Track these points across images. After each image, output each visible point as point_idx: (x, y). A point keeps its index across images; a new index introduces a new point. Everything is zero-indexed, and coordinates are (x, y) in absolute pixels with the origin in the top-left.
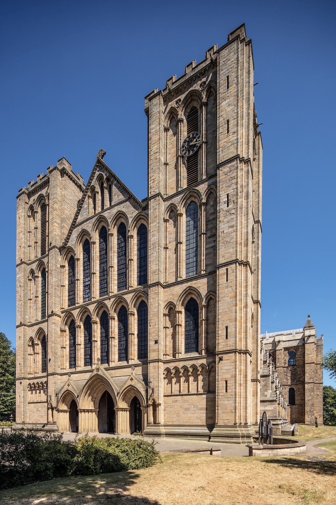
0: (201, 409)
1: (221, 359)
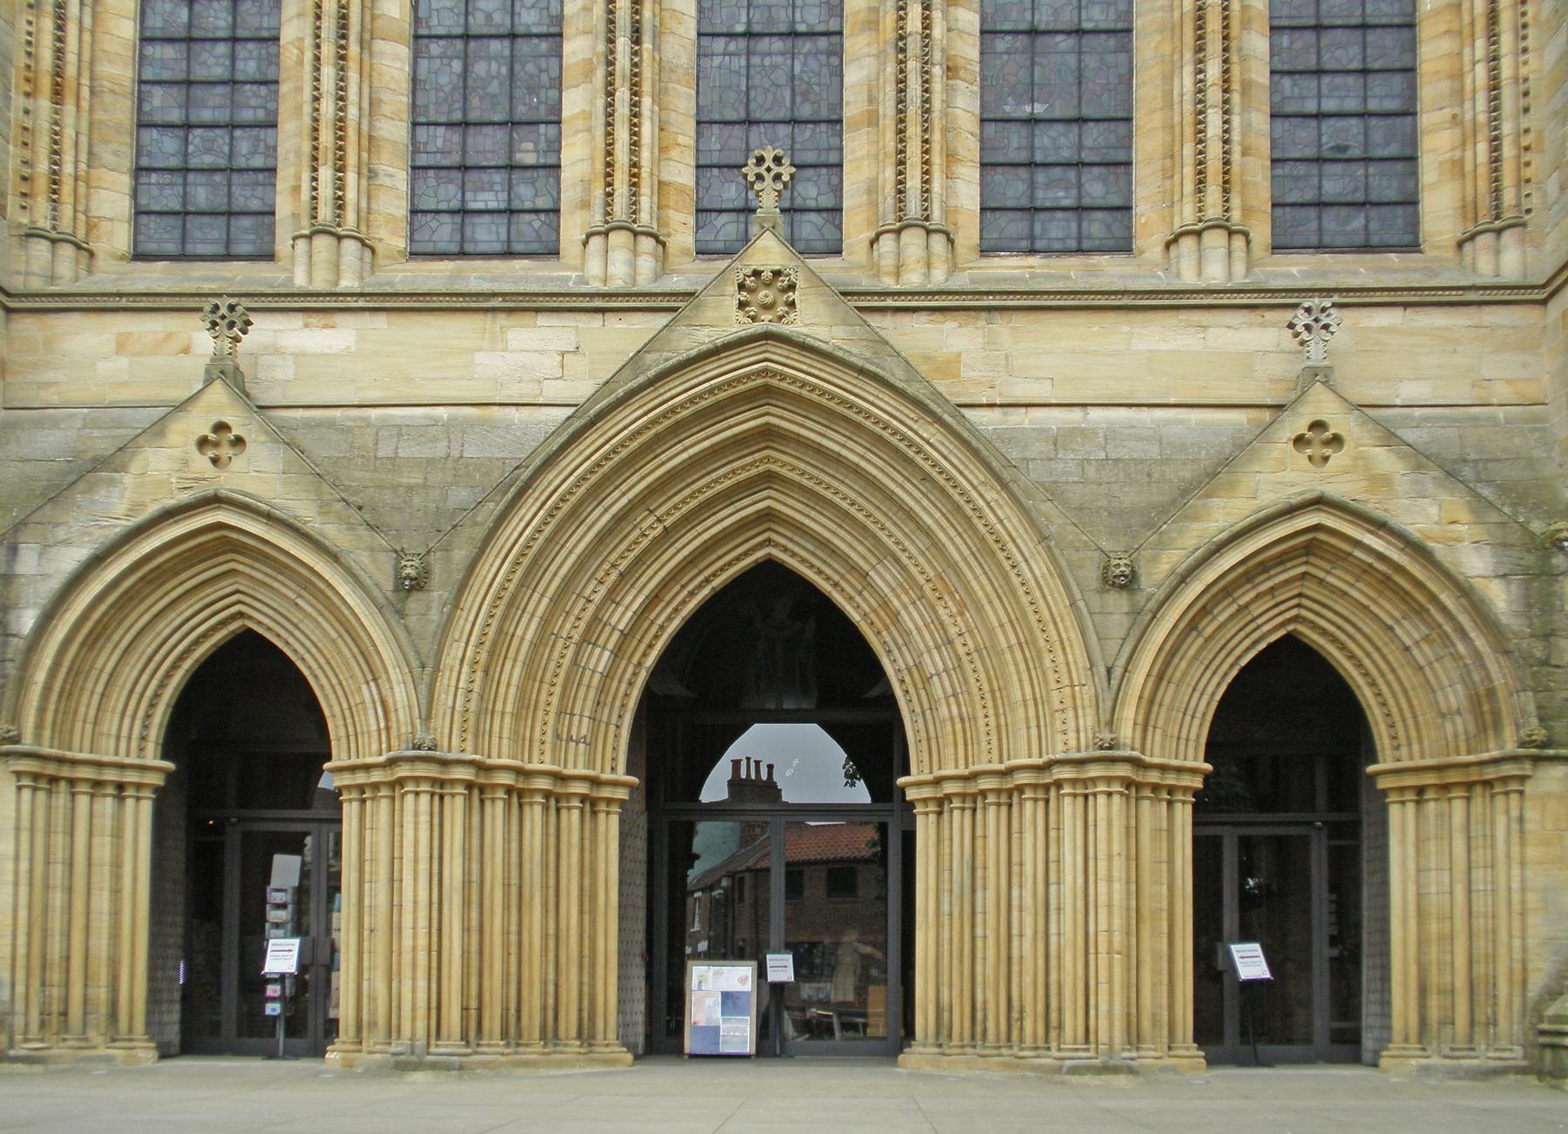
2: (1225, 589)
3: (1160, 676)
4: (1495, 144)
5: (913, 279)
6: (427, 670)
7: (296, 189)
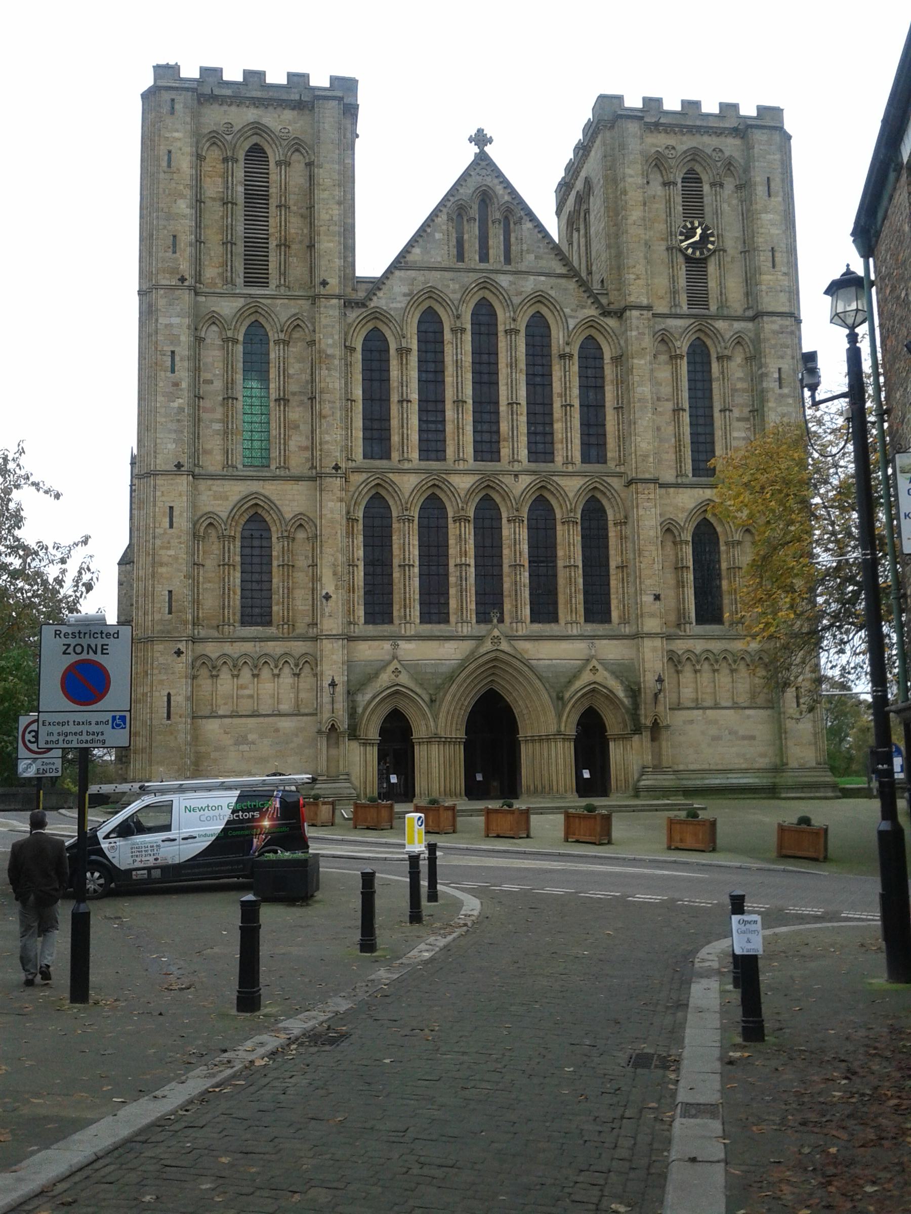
2: (579, 699)
3: (568, 716)
5: (520, 633)
6: (436, 717)
7: (399, 610)
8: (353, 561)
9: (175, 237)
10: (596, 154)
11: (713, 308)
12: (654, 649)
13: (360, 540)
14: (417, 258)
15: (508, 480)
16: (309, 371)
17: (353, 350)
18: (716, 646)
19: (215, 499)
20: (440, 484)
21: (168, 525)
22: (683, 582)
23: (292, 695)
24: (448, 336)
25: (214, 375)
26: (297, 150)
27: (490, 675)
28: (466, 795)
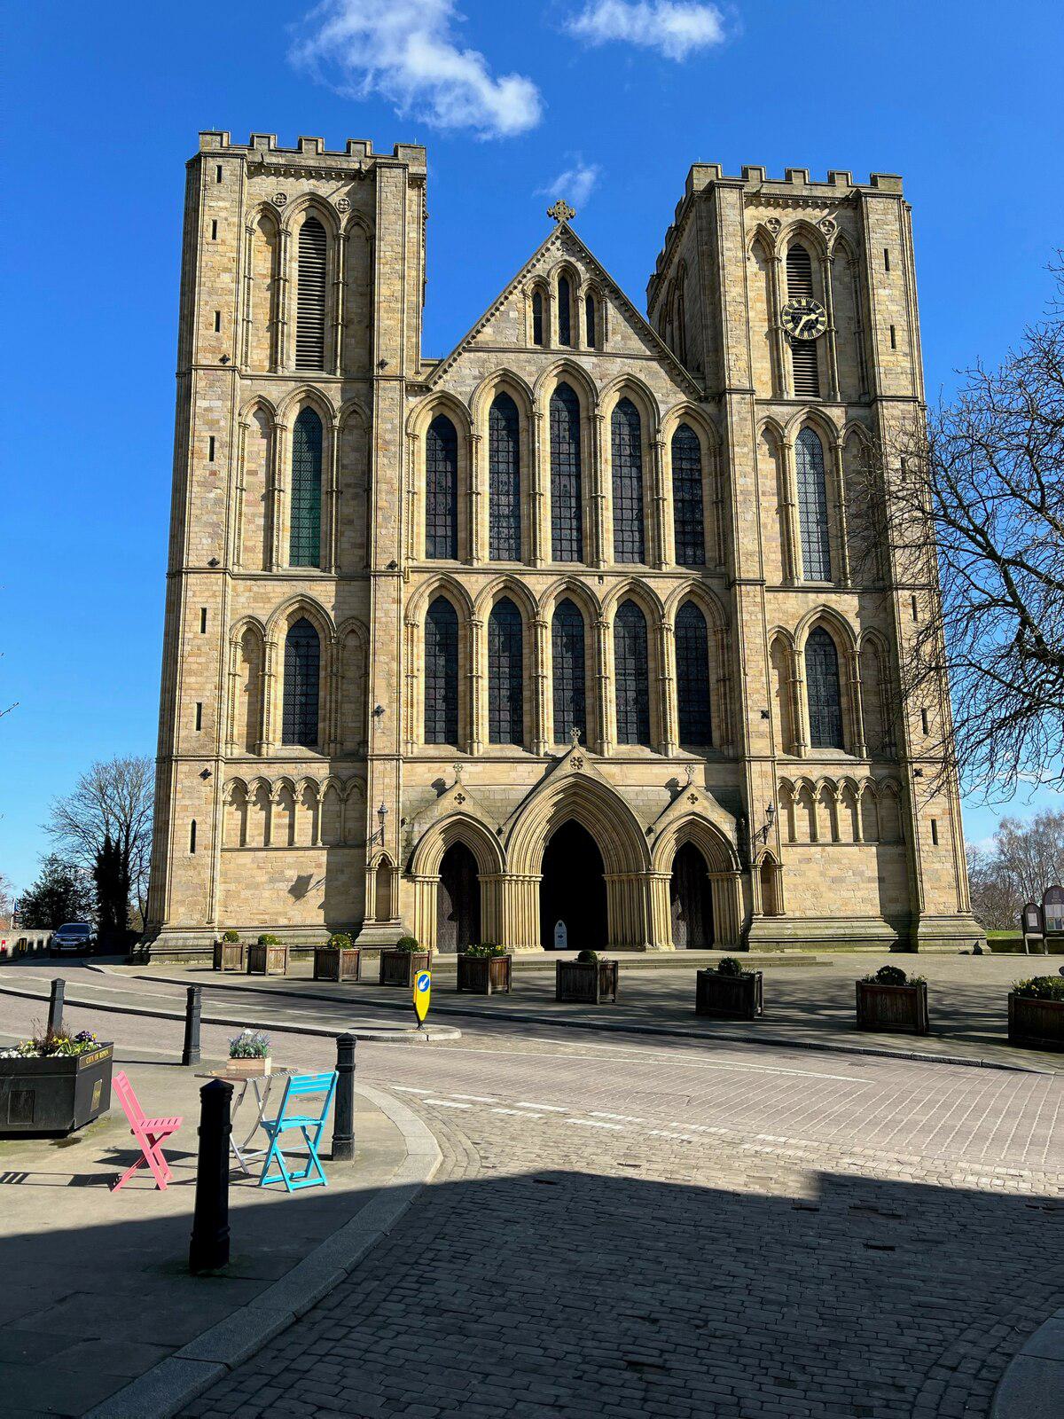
0: (870, 880)
1: (918, 773)
4: (727, 724)
7: (465, 728)
8: (412, 672)
9: (218, 314)
10: (686, 239)
11: (823, 390)
12: (763, 775)
13: (420, 648)
14: (488, 338)
15: (591, 582)
16: (365, 461)
17: (415, 437)
18: (836, 773)
19: (255, 600)
20: (513, 586)
21: (199, 629)
22: (795, 698)
23: (337, 825)
24: (523, 423)
25: (260, 465)
26: (357, 224)
27: (569, 804)
28: (542, 944)
